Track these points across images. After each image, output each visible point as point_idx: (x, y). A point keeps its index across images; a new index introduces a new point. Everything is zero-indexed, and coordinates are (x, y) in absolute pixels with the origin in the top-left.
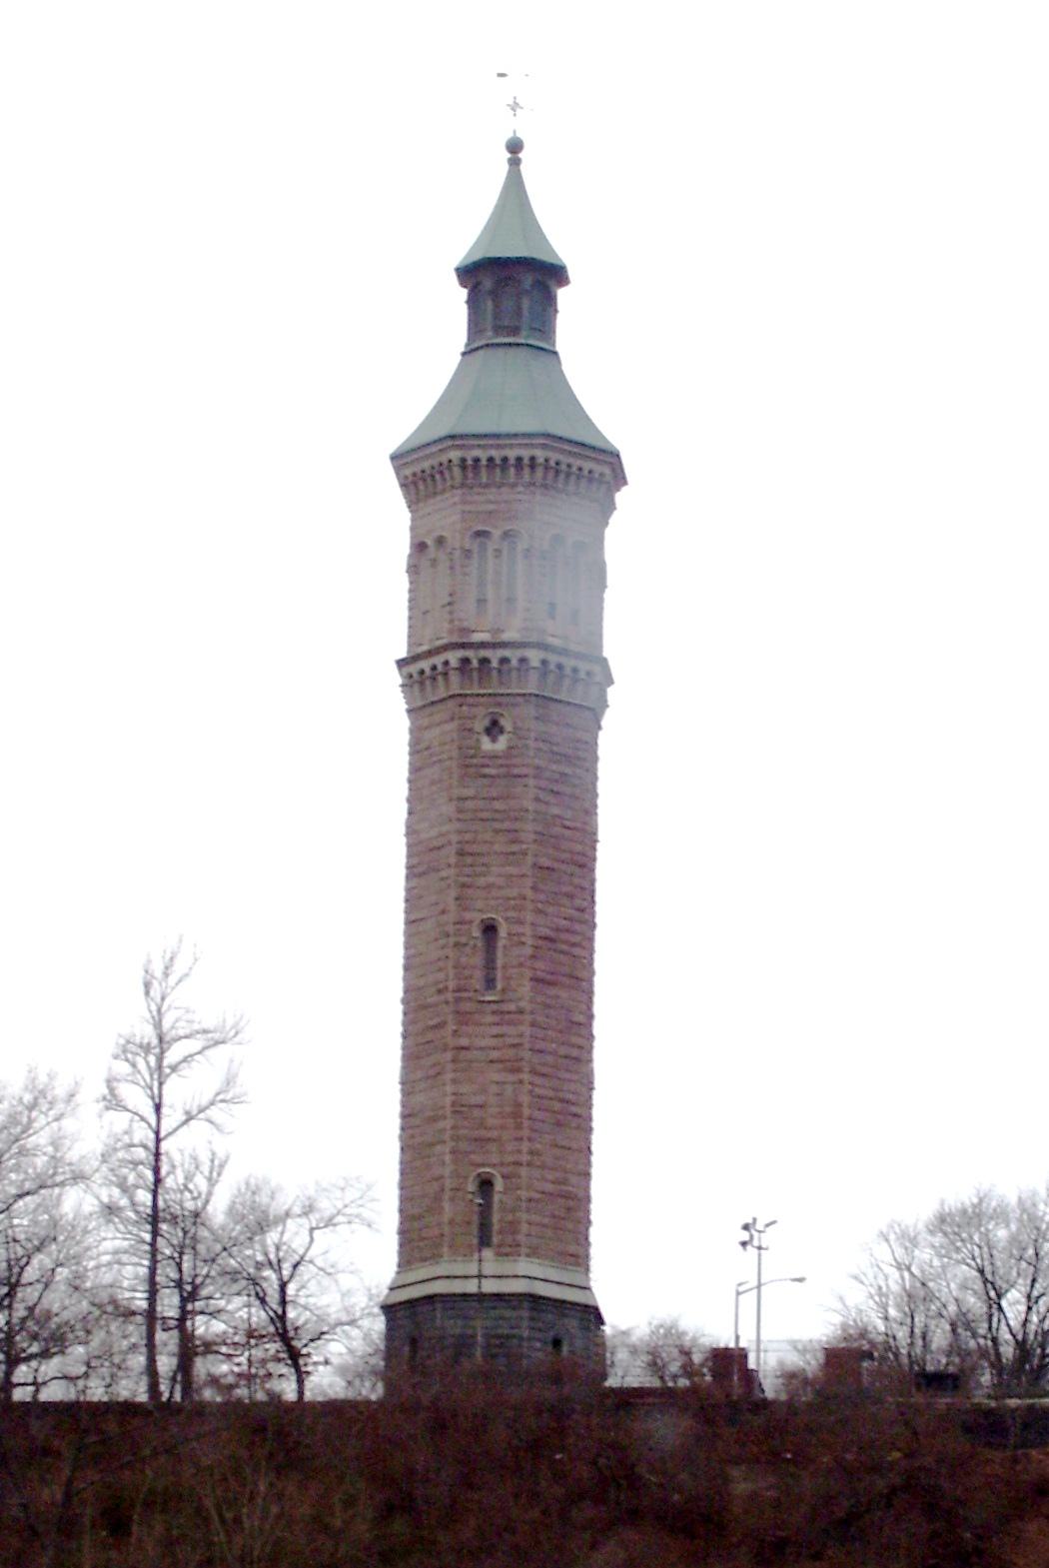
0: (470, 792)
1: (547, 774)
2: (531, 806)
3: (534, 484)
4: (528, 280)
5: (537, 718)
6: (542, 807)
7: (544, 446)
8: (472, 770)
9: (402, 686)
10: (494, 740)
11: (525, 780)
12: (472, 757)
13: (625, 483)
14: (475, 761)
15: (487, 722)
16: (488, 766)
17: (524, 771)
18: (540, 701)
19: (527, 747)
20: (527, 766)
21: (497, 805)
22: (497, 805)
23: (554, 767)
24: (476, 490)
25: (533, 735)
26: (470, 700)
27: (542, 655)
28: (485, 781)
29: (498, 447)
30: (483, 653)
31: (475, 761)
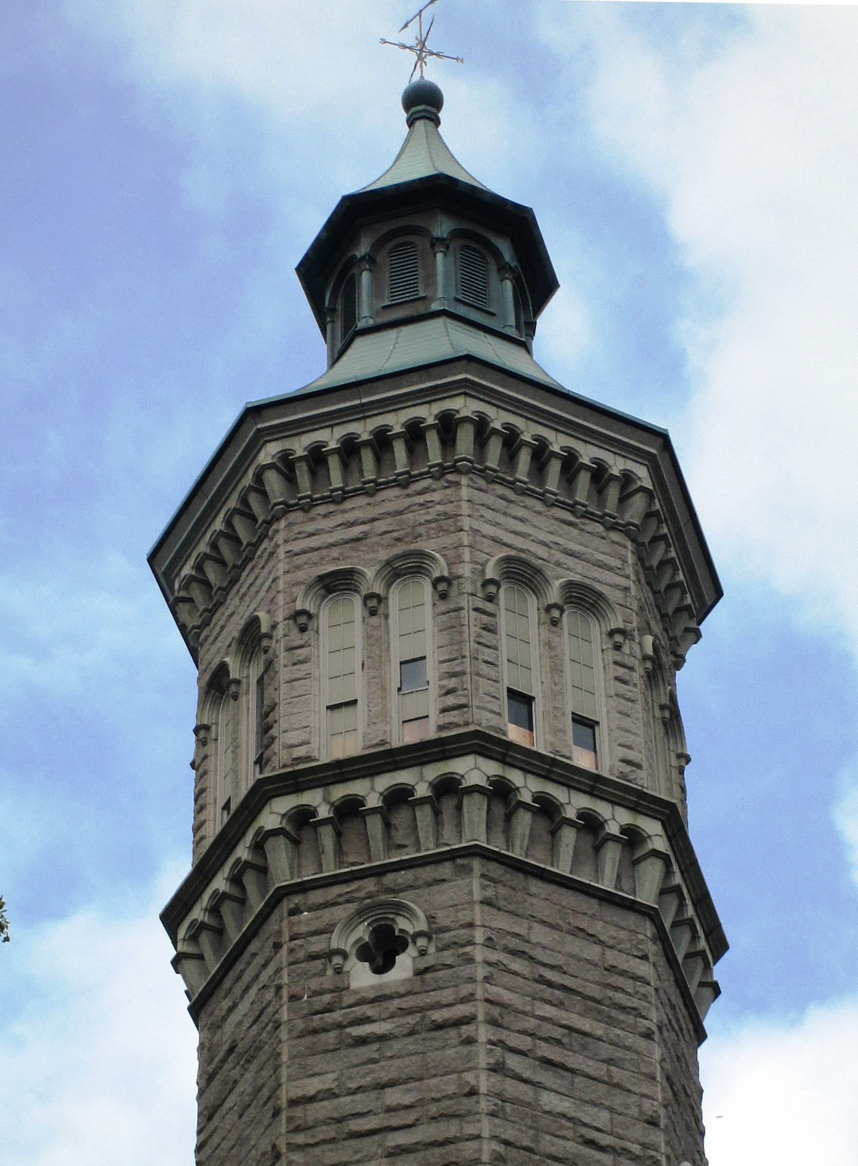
0: (313, 1086)
1: (530, 1024)
2: (484, 1082)
3: (455, 470)
4: (442, 227)
5: (487, 902)
6: (524, 1092)
7: (468, 388)
8: (331, 1037)
9: (176, 963)
10: (383, 965)
11: (466, 1030)
12: (328, 1009)
13: (718, 593)
14: (336, 1016)
15: (362, 932)
16: (368, 1020)
17: (461, 1010)
18: (495, 869)
19: (470, 960)
20: (469, 998)
21: (394, 1097)
22: (394, 1097)
23: (548, 1011)
24: (322, 510)
25: (479, 936)
26: (316, 897)
27: (492, 768)
28: (370, 1051)
29: (361, 412)
30: (339, 792)
31: (336, 1016)
